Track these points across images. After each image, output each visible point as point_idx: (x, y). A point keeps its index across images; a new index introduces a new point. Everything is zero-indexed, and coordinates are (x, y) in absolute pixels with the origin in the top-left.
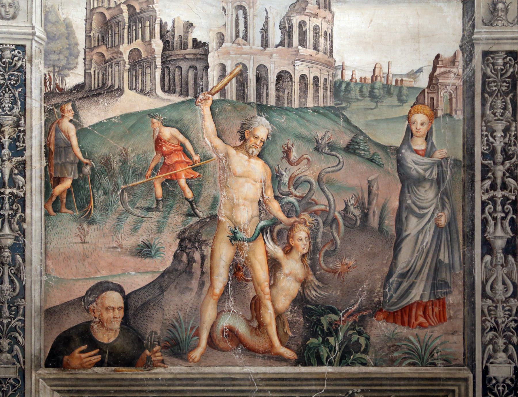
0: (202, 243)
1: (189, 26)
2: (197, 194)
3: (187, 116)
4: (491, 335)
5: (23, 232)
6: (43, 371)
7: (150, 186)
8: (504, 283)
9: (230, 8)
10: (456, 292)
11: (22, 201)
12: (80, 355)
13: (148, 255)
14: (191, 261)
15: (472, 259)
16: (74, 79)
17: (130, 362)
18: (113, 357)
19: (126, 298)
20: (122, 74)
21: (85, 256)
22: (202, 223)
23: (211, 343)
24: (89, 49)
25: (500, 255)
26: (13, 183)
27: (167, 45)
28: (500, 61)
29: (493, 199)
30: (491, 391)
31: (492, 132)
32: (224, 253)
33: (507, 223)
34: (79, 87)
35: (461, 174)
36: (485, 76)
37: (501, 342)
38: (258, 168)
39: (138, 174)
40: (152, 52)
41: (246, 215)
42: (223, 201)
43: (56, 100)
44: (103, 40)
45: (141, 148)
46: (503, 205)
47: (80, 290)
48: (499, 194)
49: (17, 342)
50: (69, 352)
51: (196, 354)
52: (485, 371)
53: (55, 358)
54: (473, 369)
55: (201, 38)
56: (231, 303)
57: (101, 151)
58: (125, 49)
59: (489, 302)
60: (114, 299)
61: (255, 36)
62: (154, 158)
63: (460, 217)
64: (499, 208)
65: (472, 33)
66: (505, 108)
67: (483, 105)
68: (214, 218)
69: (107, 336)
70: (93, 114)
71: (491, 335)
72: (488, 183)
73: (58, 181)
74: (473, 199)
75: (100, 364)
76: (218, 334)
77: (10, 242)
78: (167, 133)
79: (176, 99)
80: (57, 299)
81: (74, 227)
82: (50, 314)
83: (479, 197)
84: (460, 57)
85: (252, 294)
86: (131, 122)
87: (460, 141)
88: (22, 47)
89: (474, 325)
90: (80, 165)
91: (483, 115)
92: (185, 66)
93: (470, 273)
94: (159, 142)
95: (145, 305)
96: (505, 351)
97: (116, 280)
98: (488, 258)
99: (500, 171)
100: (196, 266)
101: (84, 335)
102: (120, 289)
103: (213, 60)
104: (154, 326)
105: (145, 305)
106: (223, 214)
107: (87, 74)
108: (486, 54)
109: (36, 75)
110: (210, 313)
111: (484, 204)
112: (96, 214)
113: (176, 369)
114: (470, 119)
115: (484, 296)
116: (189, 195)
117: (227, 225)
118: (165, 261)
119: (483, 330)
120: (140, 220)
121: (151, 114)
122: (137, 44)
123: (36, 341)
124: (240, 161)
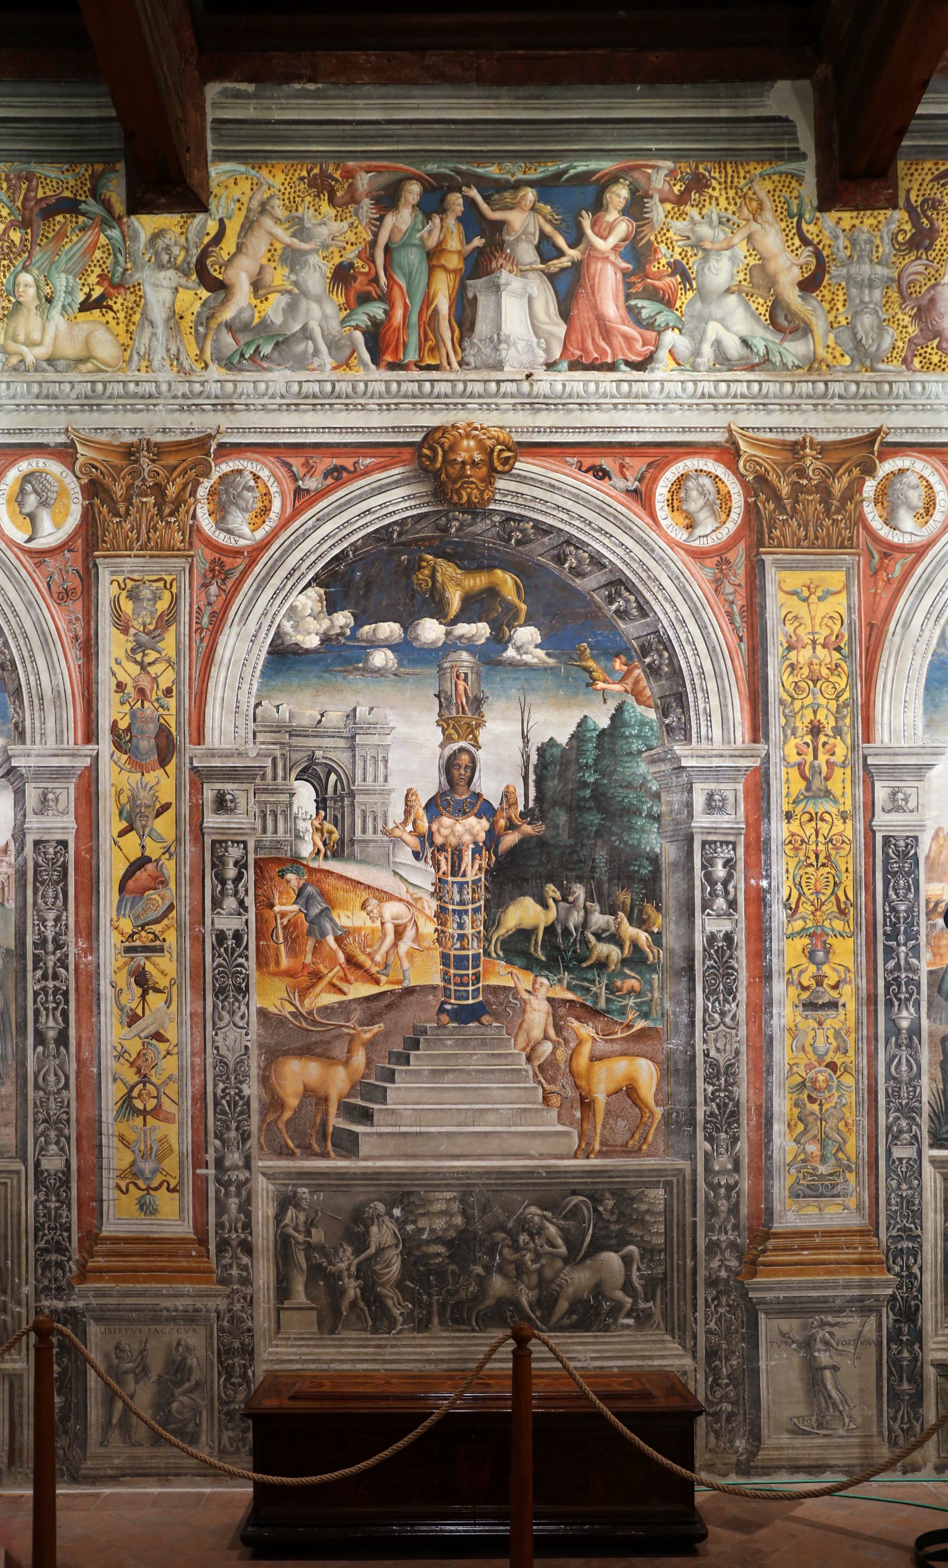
4: (42, 1127)
8: (56, 1074)
10: (8, 1083)
15: (25, 1049)
25: (52, 1046)
28: (51, 850)
29: (44, 989)
30: (43, 1183)
31: (44, 921)
33: (58, 1014)
35: (14, 964)
36: (36, 865)
37: (53, 1134)
46: (54, 995)
48: (51, 984)
52: (37, 1164)
54: (25, 1161)
59: (41, 1093)
63: (13, 1007)
64: (51, 998)
65: (24, 822)
66: (56, 898)
67: (35, 894)
71: (42, 1127)
72: (39, 973)
74: (25, 989)
83: (31, 987)
84: (12, 847)
87: (12, 930)
89: (26, 1116)
91: (35, 904)
93: (22, 1064)
96: (57, 1143)
98: (40, 1049)
99: (51, 960)
108: (37, 843)
111: (36, 994)
114: (22, 909)
115: (37, 1087)
119: (35, 1121)
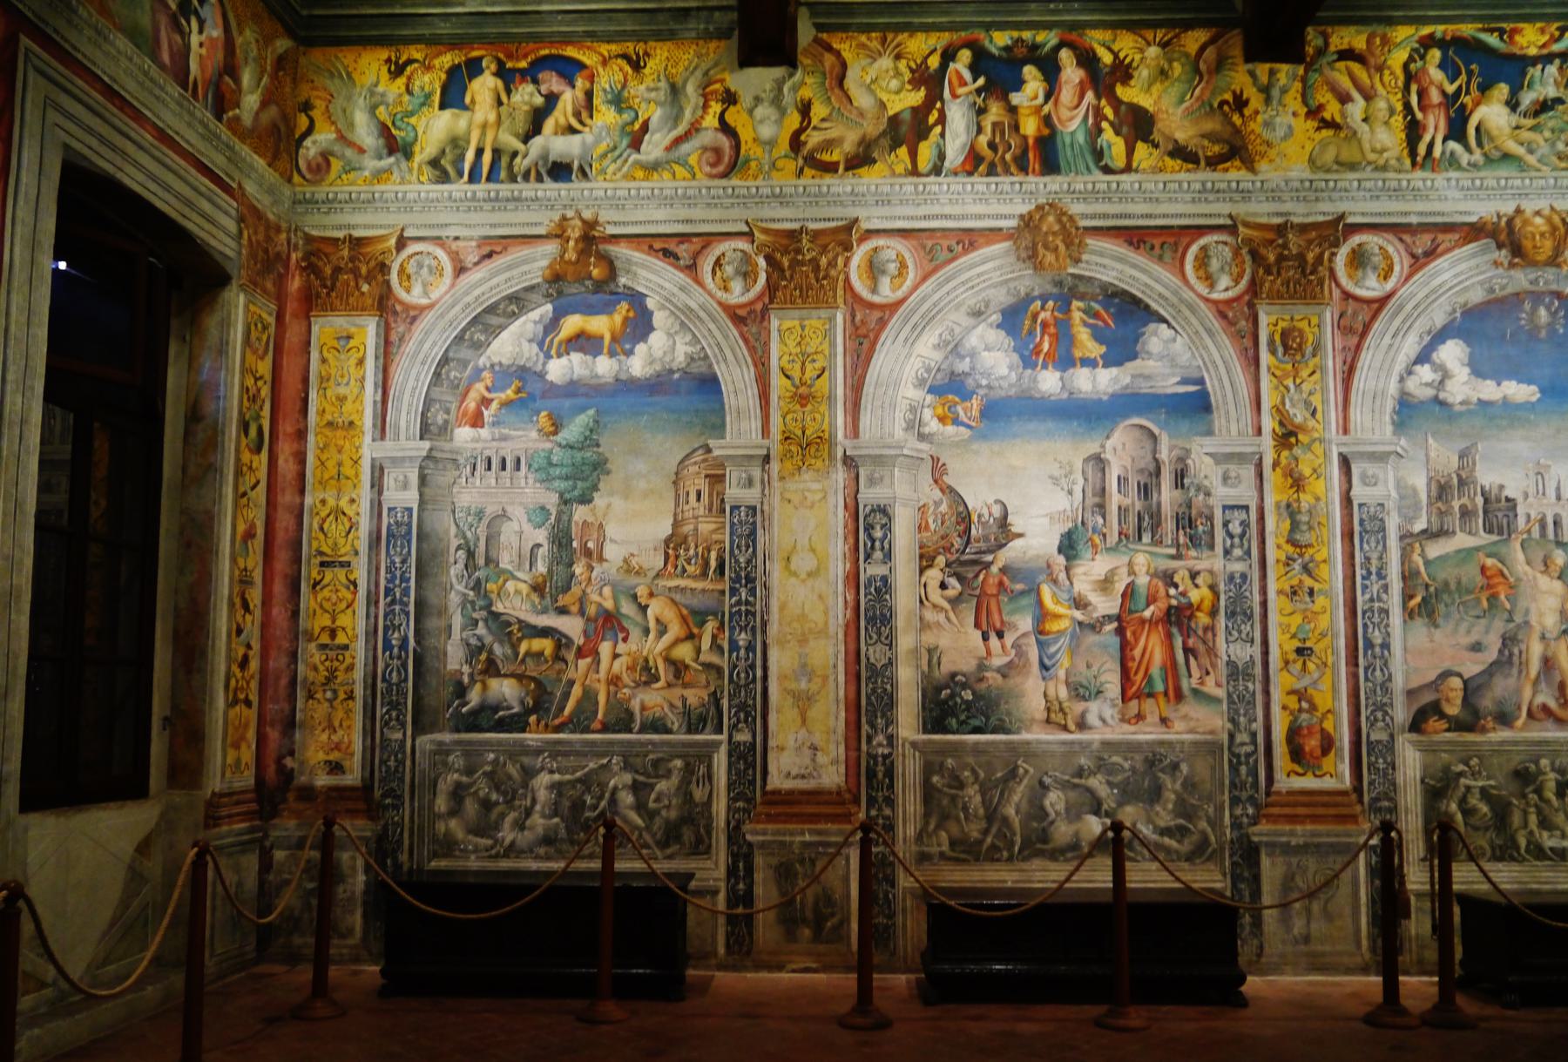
0: (1519, 641)
1: (1501, 487)
2: (1514, 605)
3: (1503, 550)
5: (1388, 634)
6: (1408, 736)
7: (1478, 600)
9: (1531, 474)
11: (1387, 612)
12: (1433, 723)
13: (1479, 650)
14: (1511, 655)
16: (1420, 526)
17: (1470, 728)
18: (1458, 725)
19: (1465, 682)
20: (1454, 521)
21: (1433, 652)
22: (1519, 627)
23: (1530, 714)
24: (1430, 504)
26: (1380, 600)
27: (1486, 501)
32: (1536, 650)
34: (1424, 532)
38: (1558, 586)
39: (1469, 592)
40: (1475, 505)
41: (1551, 621)
42: (1533, 608)
43: (1408, 541)
44: (1439, 498)
45: (1471, 574)
47: (1431, 676)
49: (1386, 713)
50: (1426, 721)
51: (1519, 723)
53: (1416, 725)
55: (1511, 495)
56: (1543, 685)
57: (1442, 575)
58: (1456, 504)
60: (1456, 683)
61: (1551, 493)
62: (1480, 580)
68: (1527, 623)
69: (1453, 709)
70: (1435, 550)
73: (1411, 597)
75: (1448, 730)
76: (1534, 709)
77: (1379, 641)
78: (1489, 562)
79: (1495, 538)
80: (1414, 684)
81: (1424, 630)
82: (1411, 694)
85: (1558, 679)
86: (1462, 555)
88: (1382, 505)
90: (1427, 586)
92: (1500, 515)
94: (1483, 569)
95: (1479, 687)
97: (1456, 669)
100: (1516, 659)
101: (1435, 709)
102: (1459, 675)
103: (1520, 510)
104: (1486, 703)
105: (1479, 687)
106: (1534, 621)
107: (1429, 521)
109: (1393, 524)
110: (1527, 693)
112: (1440, 621)
113: (1503, 734)
116: (1508, 606)
117: (1537, 629)
118: (1491, 655)
120: (1473, 625)
121: (1478, 549)
122: (1465, 500)
123: (1401, 713)
124: (1544, 582)
